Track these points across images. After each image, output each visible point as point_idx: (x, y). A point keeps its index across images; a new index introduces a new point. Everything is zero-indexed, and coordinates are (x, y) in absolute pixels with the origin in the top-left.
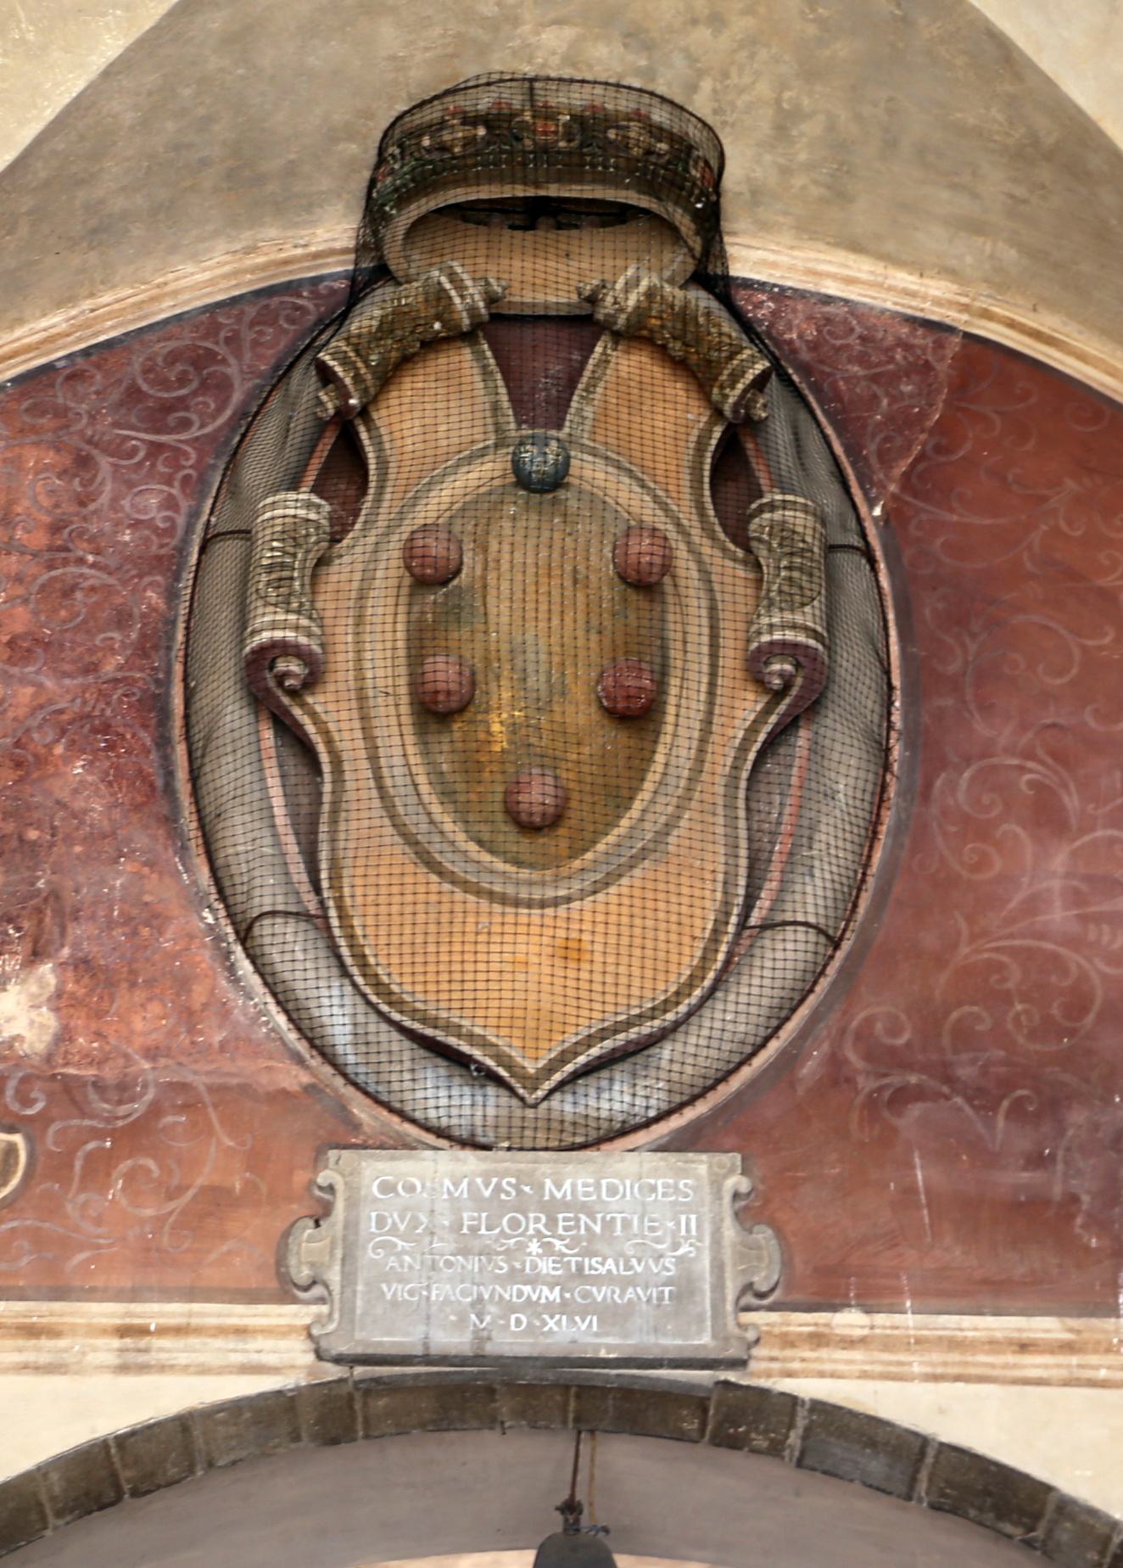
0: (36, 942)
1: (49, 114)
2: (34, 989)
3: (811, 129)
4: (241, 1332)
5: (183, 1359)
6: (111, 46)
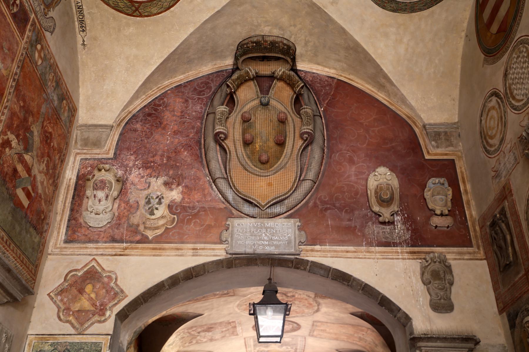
1: (181, 41)
2: (178, 191)
3: (311, 44)
4: (213, 249)
5: (204, 254)
6: (191, 30)
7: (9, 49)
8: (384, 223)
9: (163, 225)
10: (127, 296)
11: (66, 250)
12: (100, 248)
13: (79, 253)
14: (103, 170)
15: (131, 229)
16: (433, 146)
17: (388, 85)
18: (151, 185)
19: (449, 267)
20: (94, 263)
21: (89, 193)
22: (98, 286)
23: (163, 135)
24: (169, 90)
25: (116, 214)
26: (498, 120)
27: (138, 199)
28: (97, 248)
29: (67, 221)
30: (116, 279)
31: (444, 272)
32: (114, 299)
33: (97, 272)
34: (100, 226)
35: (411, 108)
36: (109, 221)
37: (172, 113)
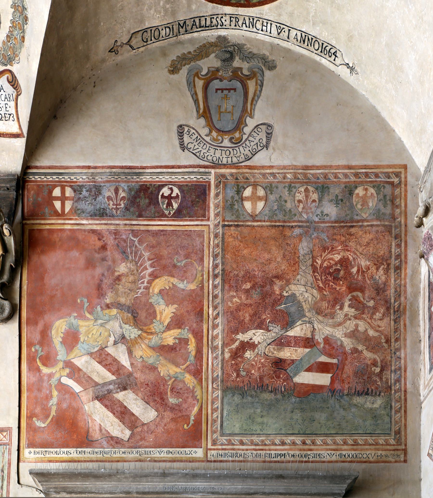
7: (187, 256)
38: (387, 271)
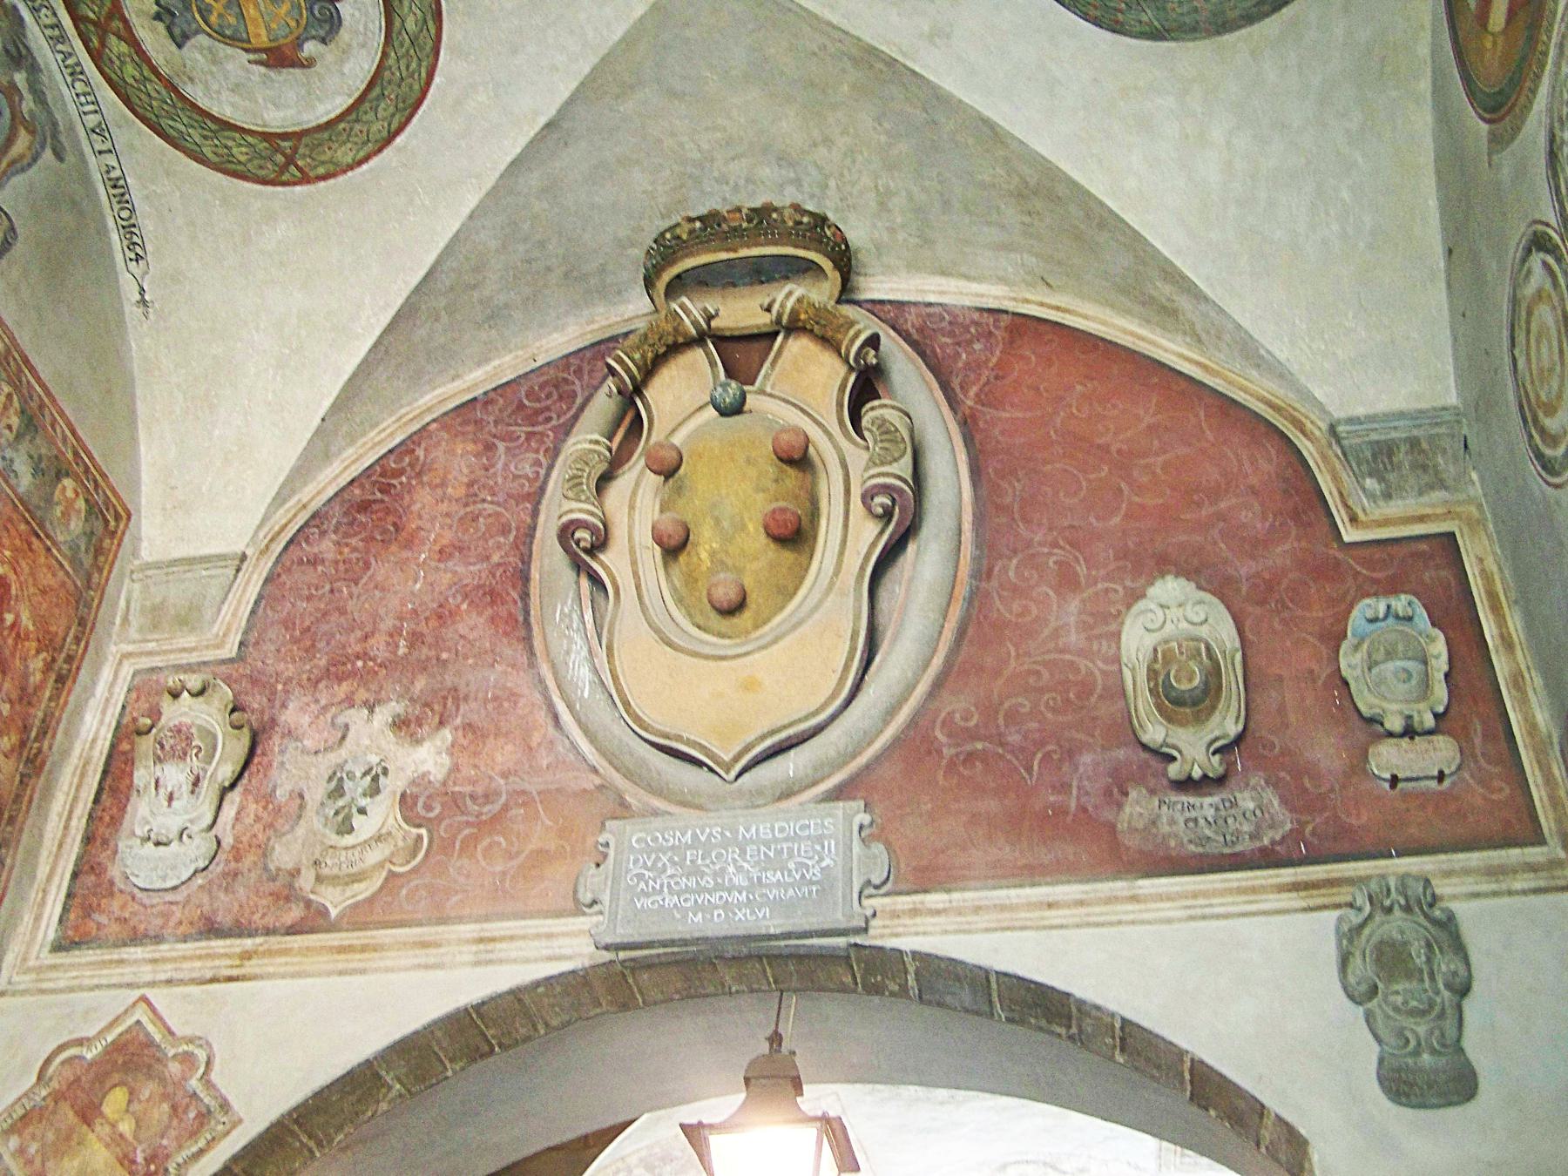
0: (442, 716)
1: (442, 245)
2: (439, 743)
3: (897, 202)
4: (550, 936)
5: (513, 954)
6: (472, 200)
8: (1186, 784)
9: (381, 865)
10: (241, 1121)
11: (54, 975)
12: (164, 960)
13: (96, 981)
14: (186, 694)
15: (272, 886)
16: (1371, 496)
17: (1184, 303)
18: (351, 735)
19: (1449, 925)
20: (141, 1014)
21: (141, 776)
22: (145, 1094)
23: (402, 565)
24: (434, 420)
25: (228, 841)
26: (1559, 332)
27: (303, 785)
28: (154, 961)
29: (68, 876)
30: (208, 1063)
31: (1429, 945)
32: (194, 1134)
33: (150, 1043)
34: (169, 884)
35: (1281, 373)
36: (202, 865)
37: (439, 491)
38: (48, 667)
